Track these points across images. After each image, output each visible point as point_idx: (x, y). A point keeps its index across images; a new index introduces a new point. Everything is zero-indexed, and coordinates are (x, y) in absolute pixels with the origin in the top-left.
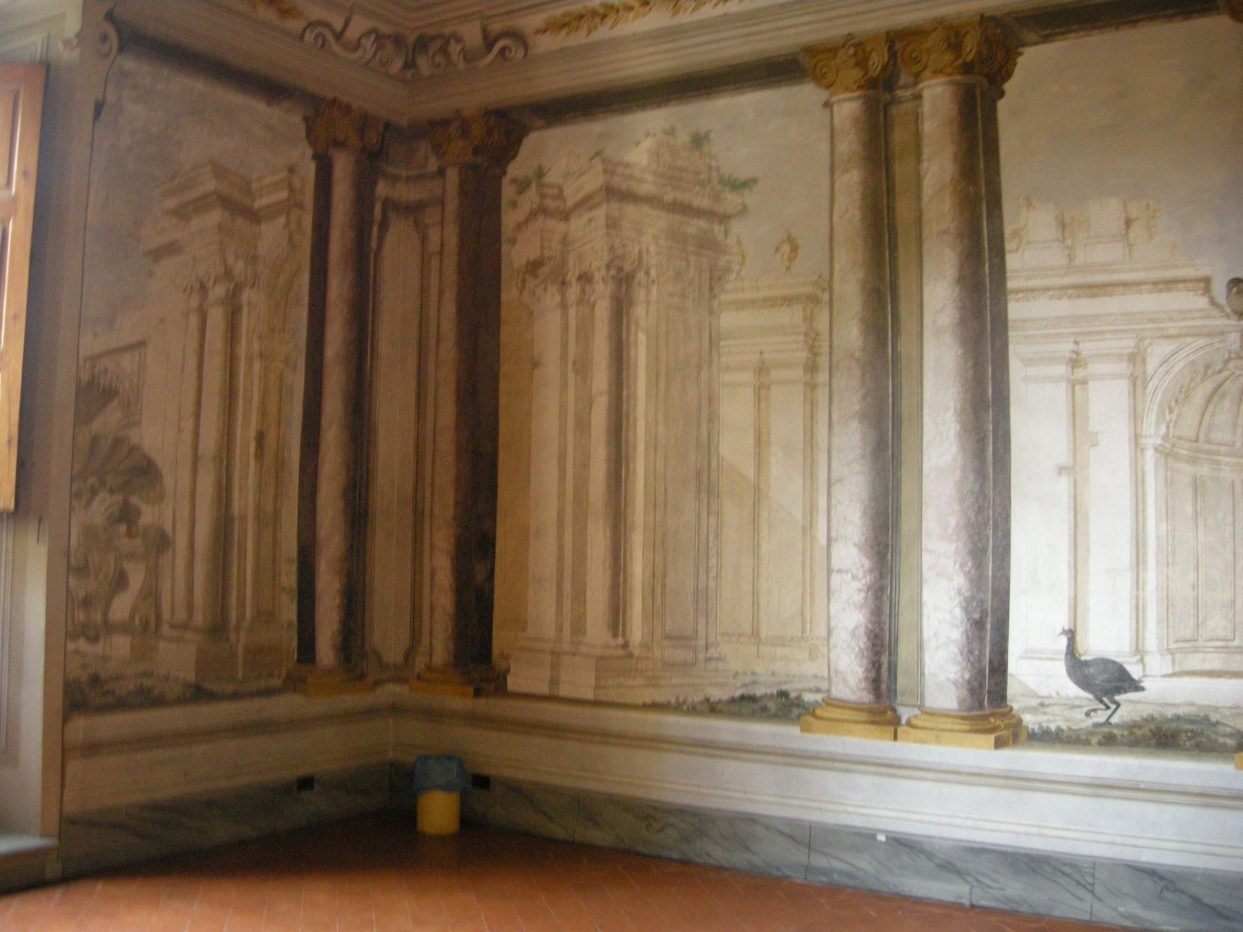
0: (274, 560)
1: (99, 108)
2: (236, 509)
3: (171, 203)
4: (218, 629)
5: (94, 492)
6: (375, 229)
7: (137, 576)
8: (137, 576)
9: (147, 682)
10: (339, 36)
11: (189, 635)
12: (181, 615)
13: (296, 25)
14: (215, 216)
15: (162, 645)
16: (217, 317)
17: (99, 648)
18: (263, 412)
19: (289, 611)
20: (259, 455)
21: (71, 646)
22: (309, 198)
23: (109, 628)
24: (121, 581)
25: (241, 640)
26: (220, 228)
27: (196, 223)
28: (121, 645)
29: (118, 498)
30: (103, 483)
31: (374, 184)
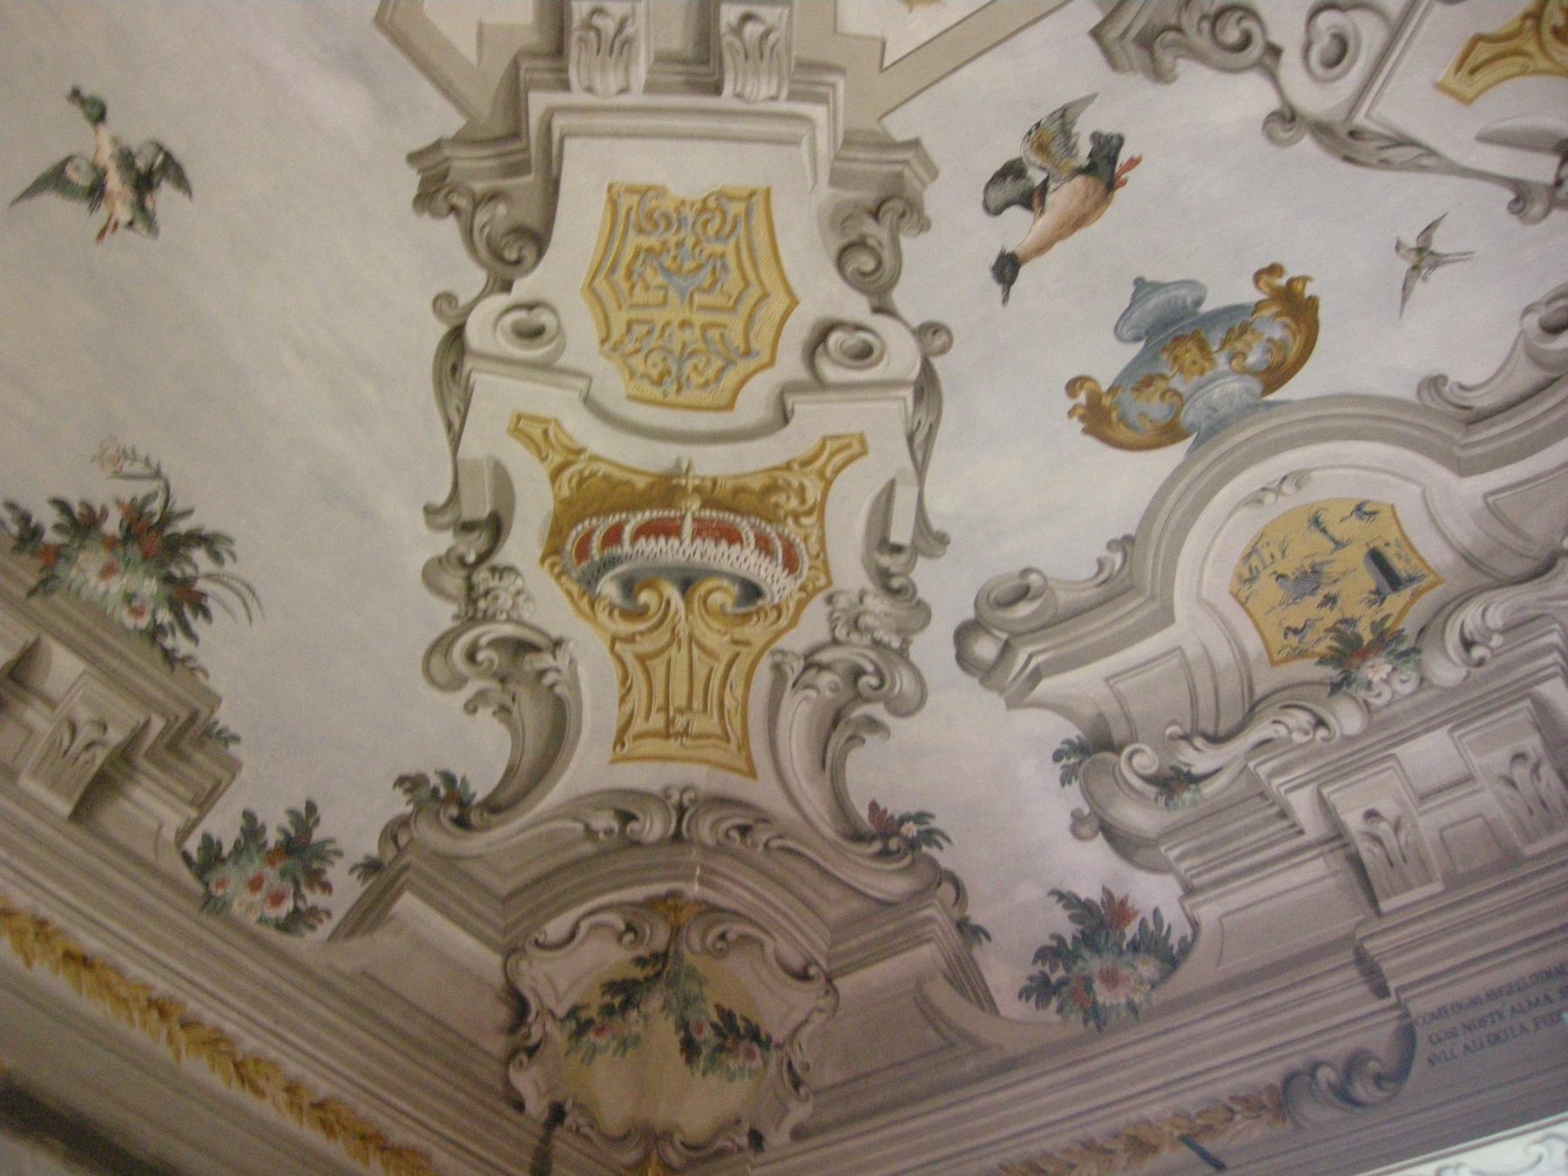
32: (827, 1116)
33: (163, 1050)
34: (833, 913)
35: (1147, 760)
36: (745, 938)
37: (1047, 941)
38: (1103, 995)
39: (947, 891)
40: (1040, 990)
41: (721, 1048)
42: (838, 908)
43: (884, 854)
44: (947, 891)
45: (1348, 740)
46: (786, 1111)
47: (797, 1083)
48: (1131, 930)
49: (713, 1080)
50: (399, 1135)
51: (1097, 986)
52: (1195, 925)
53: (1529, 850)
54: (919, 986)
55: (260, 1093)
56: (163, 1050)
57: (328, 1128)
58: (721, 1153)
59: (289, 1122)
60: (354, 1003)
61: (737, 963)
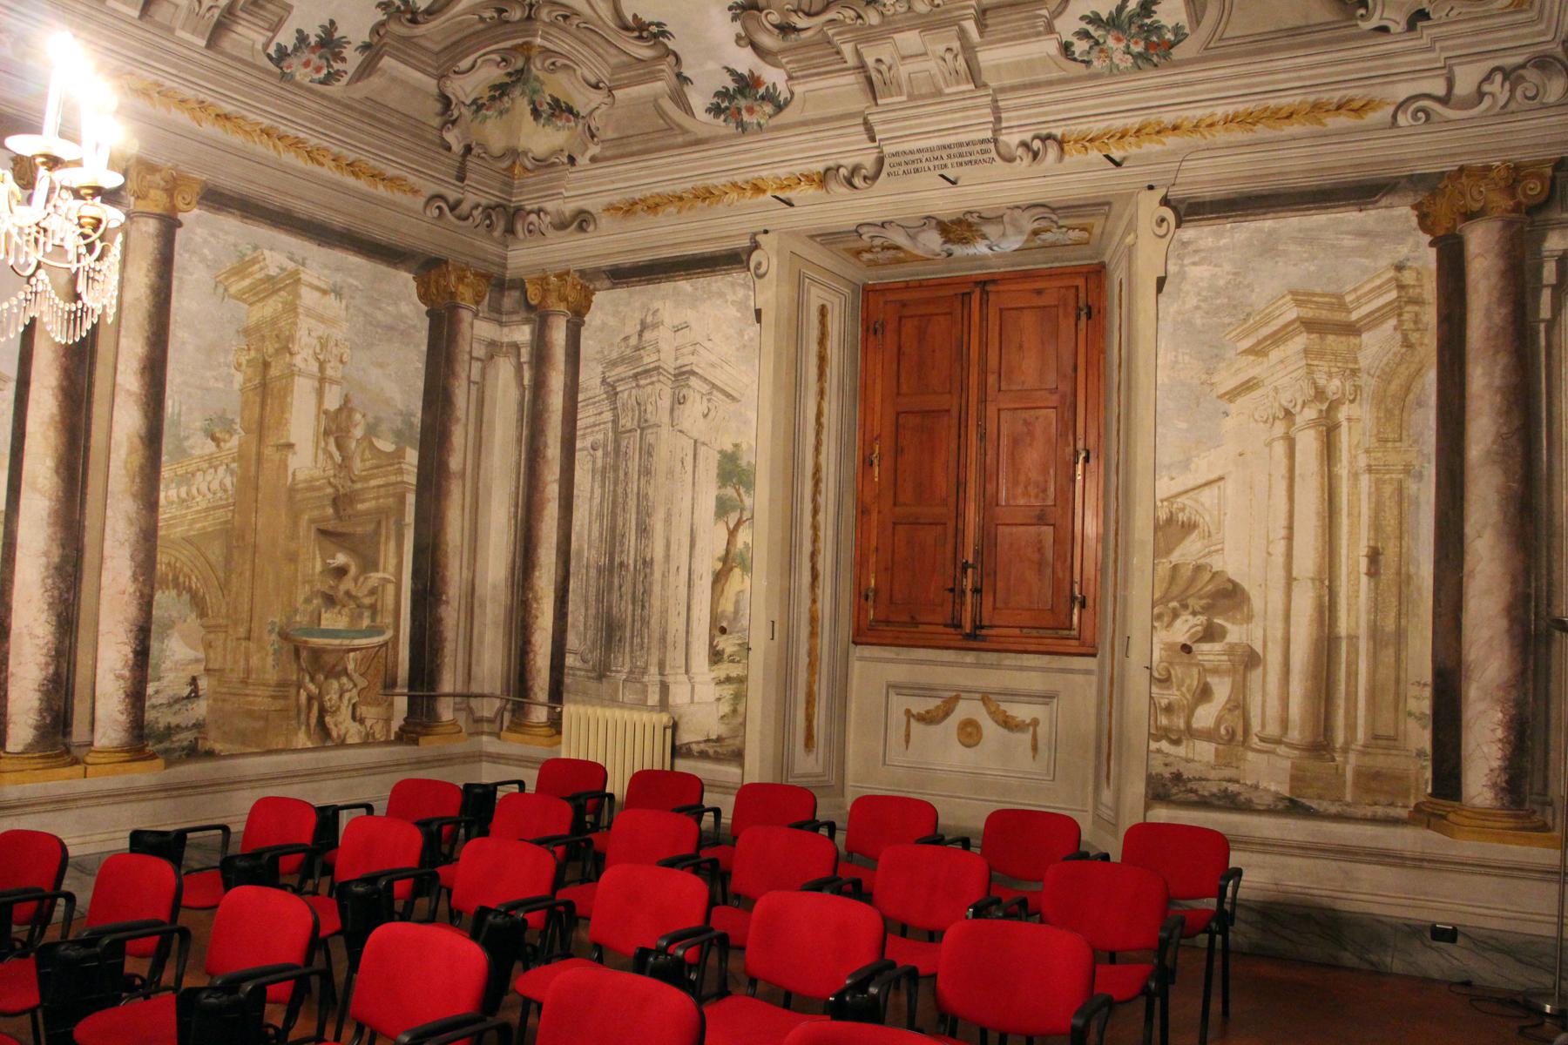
0: (1398, 681)
1: (1161, 283)
2: (1343, 628)
3: (1246, 344)
4: (1320, 746)
5: (1175, 615)
6: (1546, 296)
7: (1222, 690)
8: (1222, 690)
9: (1233, 787)
10: (1444, 101)
11: (1282, 750)
12: (1273, 730)
13: (1382, 115)
14: (1301, 341)
15: (1250, 755)
16: (1308, 443)
17: (1181, 751)
18: (1377, 526)
19: (1421, 738)
20: (1374, 571)
21: (1154, 746)
22: (1430, 290)
23: (1191, 733)
24: (1205, 693)
25: (1351, 765)
26: (1306, 351)
27: (1275, 354)
28: (1205, 751)
29: (1202, 619)
30: (1185, 607)
31: (1543, 238)
32: (608, 153)
33: (272, 153)
34: (613, 61)
35: (775, 18)
36: (566, 66)
37: (721, 89)
38: (746, 117)
39: (671, 59)
40: (716, 110)
41: (553, 115)
42: (615, 59)
43: (640, 38)
44: (671, 59)
45: (871, 26)
46: (587, 148)
47: (593, 136)
48: (762, 91)
49: (549, 129)
50: (391, 171)
51: (744, 112)
52: (792, 94)
53: (947, 91)
54: (656, 100)
55: (322, 165)
56: (272, 153)
57: (353, 173)
58: (554, 164)
59: (337, 176)
60: (362, 113)
61: (561, 77)
